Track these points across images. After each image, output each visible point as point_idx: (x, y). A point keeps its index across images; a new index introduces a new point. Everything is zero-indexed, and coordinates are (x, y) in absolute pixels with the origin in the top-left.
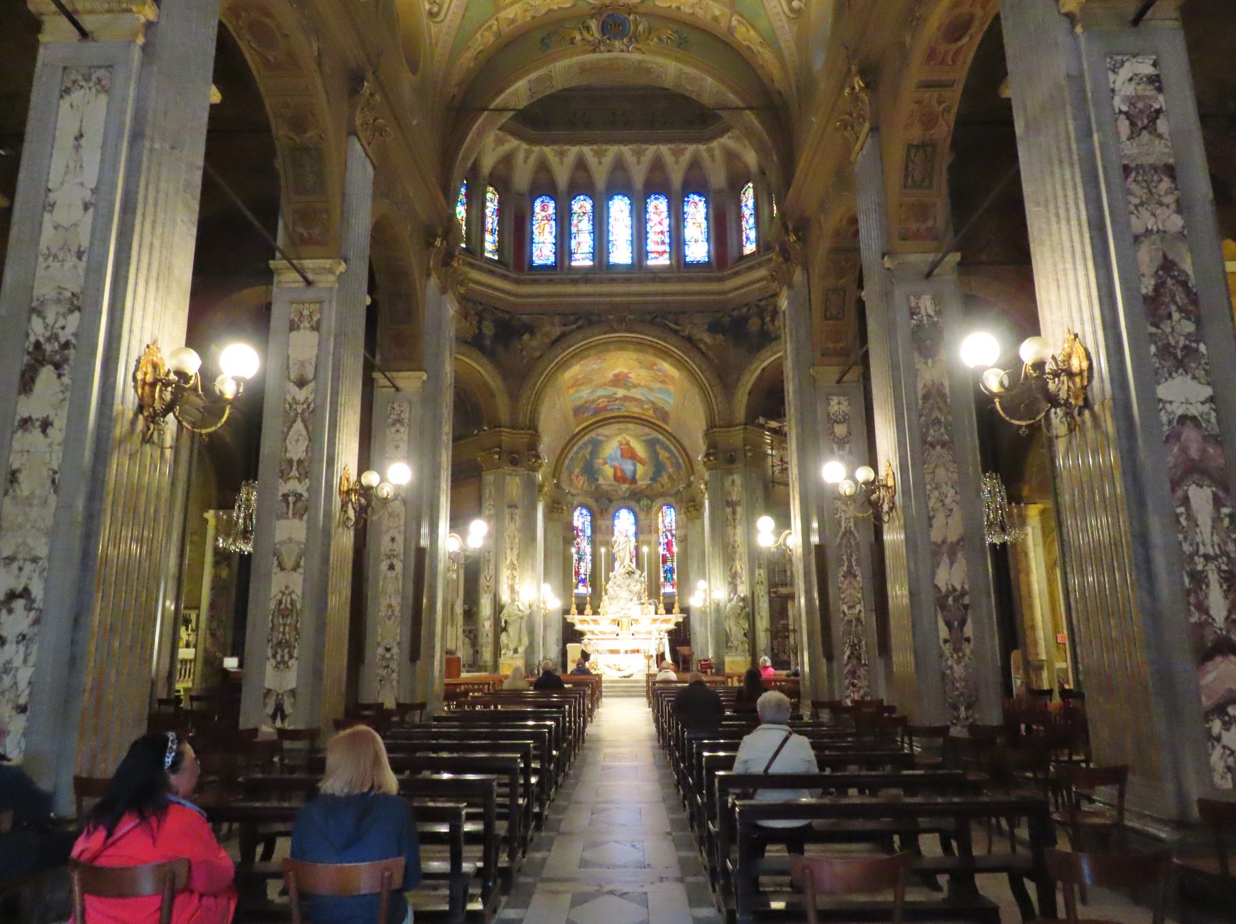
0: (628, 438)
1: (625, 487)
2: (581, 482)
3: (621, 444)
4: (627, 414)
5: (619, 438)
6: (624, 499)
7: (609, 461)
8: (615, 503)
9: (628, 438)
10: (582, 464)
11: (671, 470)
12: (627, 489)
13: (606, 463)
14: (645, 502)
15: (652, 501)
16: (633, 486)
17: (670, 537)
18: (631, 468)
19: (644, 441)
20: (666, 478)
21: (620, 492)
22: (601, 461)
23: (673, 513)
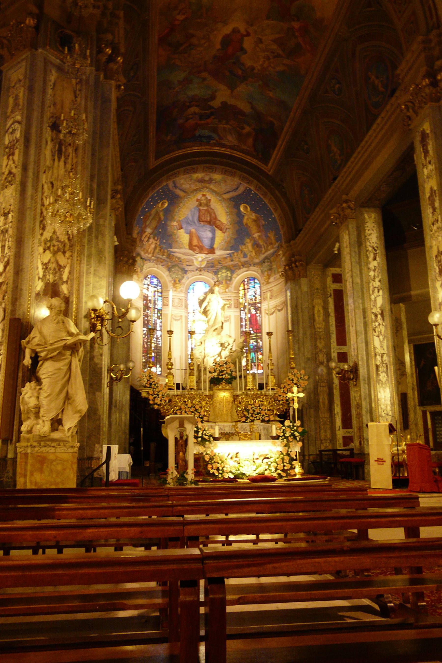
0: (209, 196)
1: (201, 257)
2: (153, 246)
3: (200, 205)
4: (217, 149)
5: (199, 196)
6: (200, 270)
7: (184, 226)
8: (189, 274)
9: (209, 196)
10: (154, 224)
11: (256, 235)
12: (203, 260)
13: (181, 228)
14: (223, 274)
15: (232, 272)
16: (210, 257)
17: (253, 312)
18: (210, 235)
19: (231, 199)
20: (249, 245)
21: (196, 263)
22: (175, 224)
23: (257, 285)
